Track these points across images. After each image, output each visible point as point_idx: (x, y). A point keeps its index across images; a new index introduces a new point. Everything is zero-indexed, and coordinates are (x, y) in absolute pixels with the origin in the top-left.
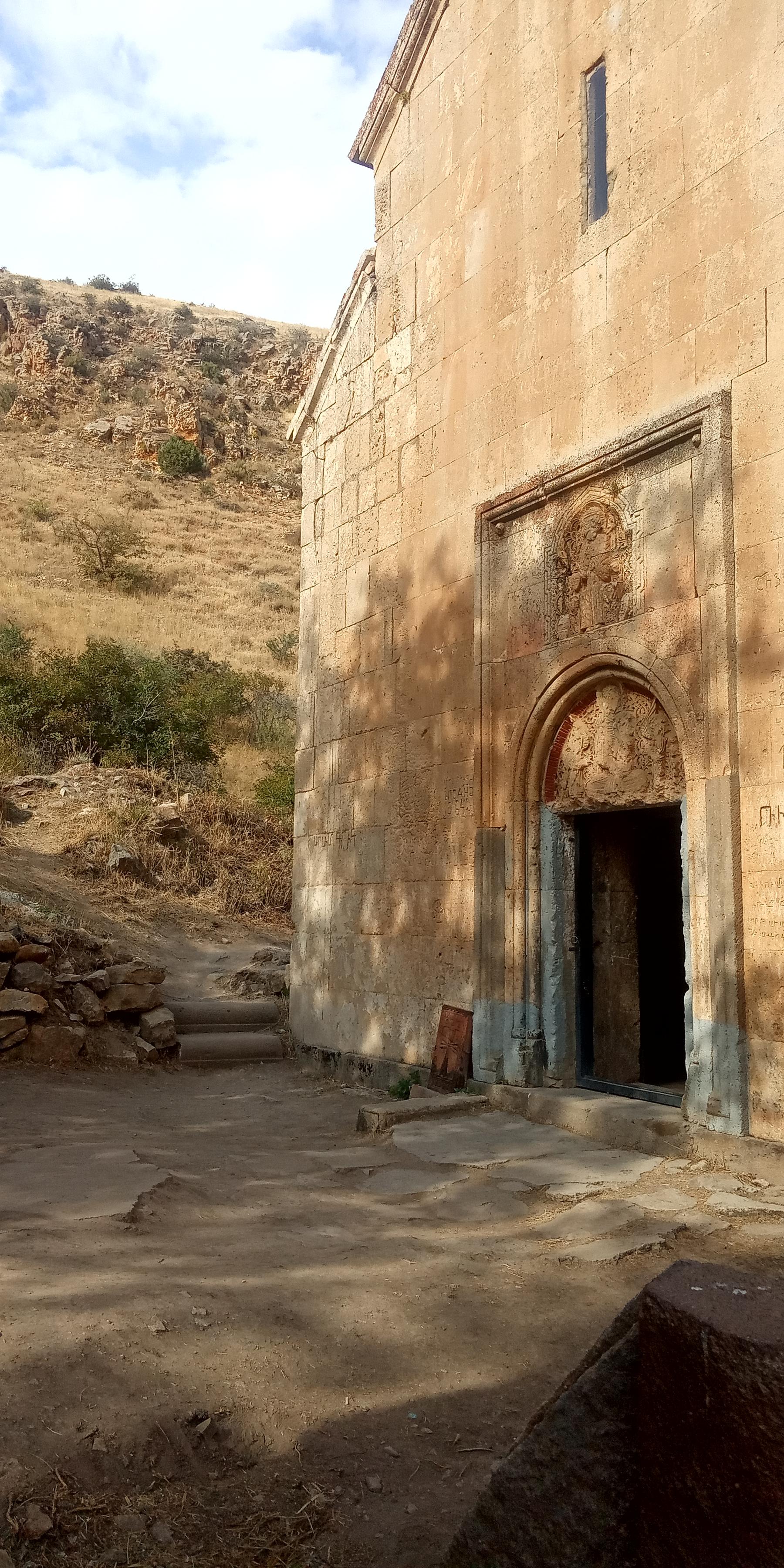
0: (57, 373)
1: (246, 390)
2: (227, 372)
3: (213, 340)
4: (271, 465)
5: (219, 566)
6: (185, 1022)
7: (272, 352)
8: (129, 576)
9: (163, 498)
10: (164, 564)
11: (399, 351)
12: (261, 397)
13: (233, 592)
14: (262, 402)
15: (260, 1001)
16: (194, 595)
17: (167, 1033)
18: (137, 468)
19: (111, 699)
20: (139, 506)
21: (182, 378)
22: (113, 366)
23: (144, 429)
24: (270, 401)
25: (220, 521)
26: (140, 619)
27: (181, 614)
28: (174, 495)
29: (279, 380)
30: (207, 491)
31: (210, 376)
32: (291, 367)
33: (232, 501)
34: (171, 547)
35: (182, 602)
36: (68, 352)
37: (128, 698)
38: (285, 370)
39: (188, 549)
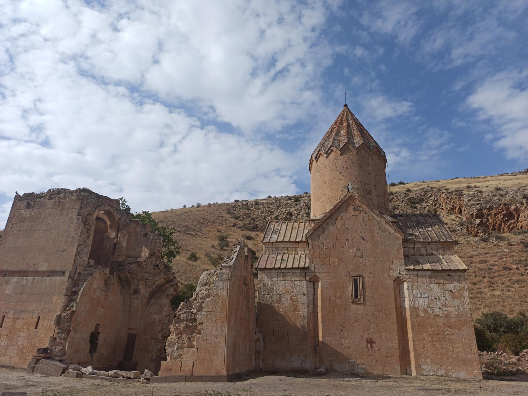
29: (432, 204)
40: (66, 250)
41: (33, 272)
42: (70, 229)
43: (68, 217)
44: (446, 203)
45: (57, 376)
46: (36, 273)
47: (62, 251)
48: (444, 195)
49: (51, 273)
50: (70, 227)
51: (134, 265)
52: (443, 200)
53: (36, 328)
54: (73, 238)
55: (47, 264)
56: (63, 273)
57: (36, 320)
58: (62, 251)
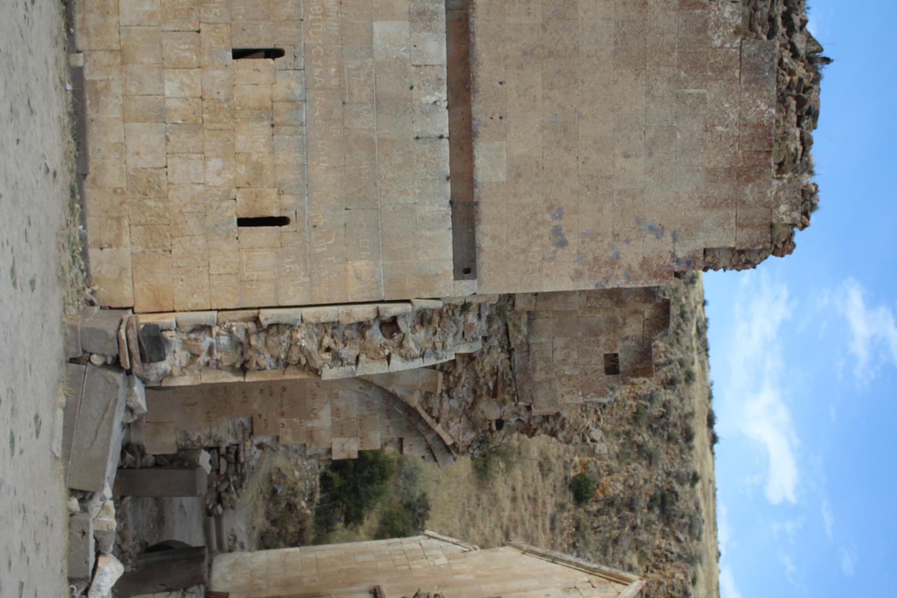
0: (630, 402)
1: (647, 525)
2: (657, 511)
3: (677, 499)
4: (592, 548)
5: (505, 521)
6: (219, 518)
7: (678, 540)
8: (485, 466)
9: (551, 480)
10: (501, 487)
11: (443, 561)
12: (644, 536)
13: (487, 531)
14: (640, 538)
15: (226, 544)
16: (481, 507)
17: (215, 512)
18: (572, 460)
19: (366, 474)
20: (541, 465)
21: (642, 482)
22: (644, 436)
23: (599, 462)
24: (643, 543)
25: (540, 518)
26: (456, 477)
27: (465, 501)
28: (555, 486)
29: (659, 548)
30: (562, 507)
31: (651, 500)
32: (669, 555)
33: (558, 524)
34: (514, 489)
35: (473, 501)
36: (646, 407)
37: (370, 480)
38: (667, 551)
39: (514, 500)
40: (562, 244)
41: (468, 119)
42: (650, 238)
43: (701, 213)
44: (660, 583)
45: (67, 474)
46: (463, 138)
47: (557, 231)
48: (682, 577)
49: (465, 213)
50: (658, 231)
51: (503, 356)
52: (668, 574)
53: (243, 222)
54: (613, 262)
55: (502, 177)
56: (466, 268)
57: (275, 213)
58: (557, 231)
